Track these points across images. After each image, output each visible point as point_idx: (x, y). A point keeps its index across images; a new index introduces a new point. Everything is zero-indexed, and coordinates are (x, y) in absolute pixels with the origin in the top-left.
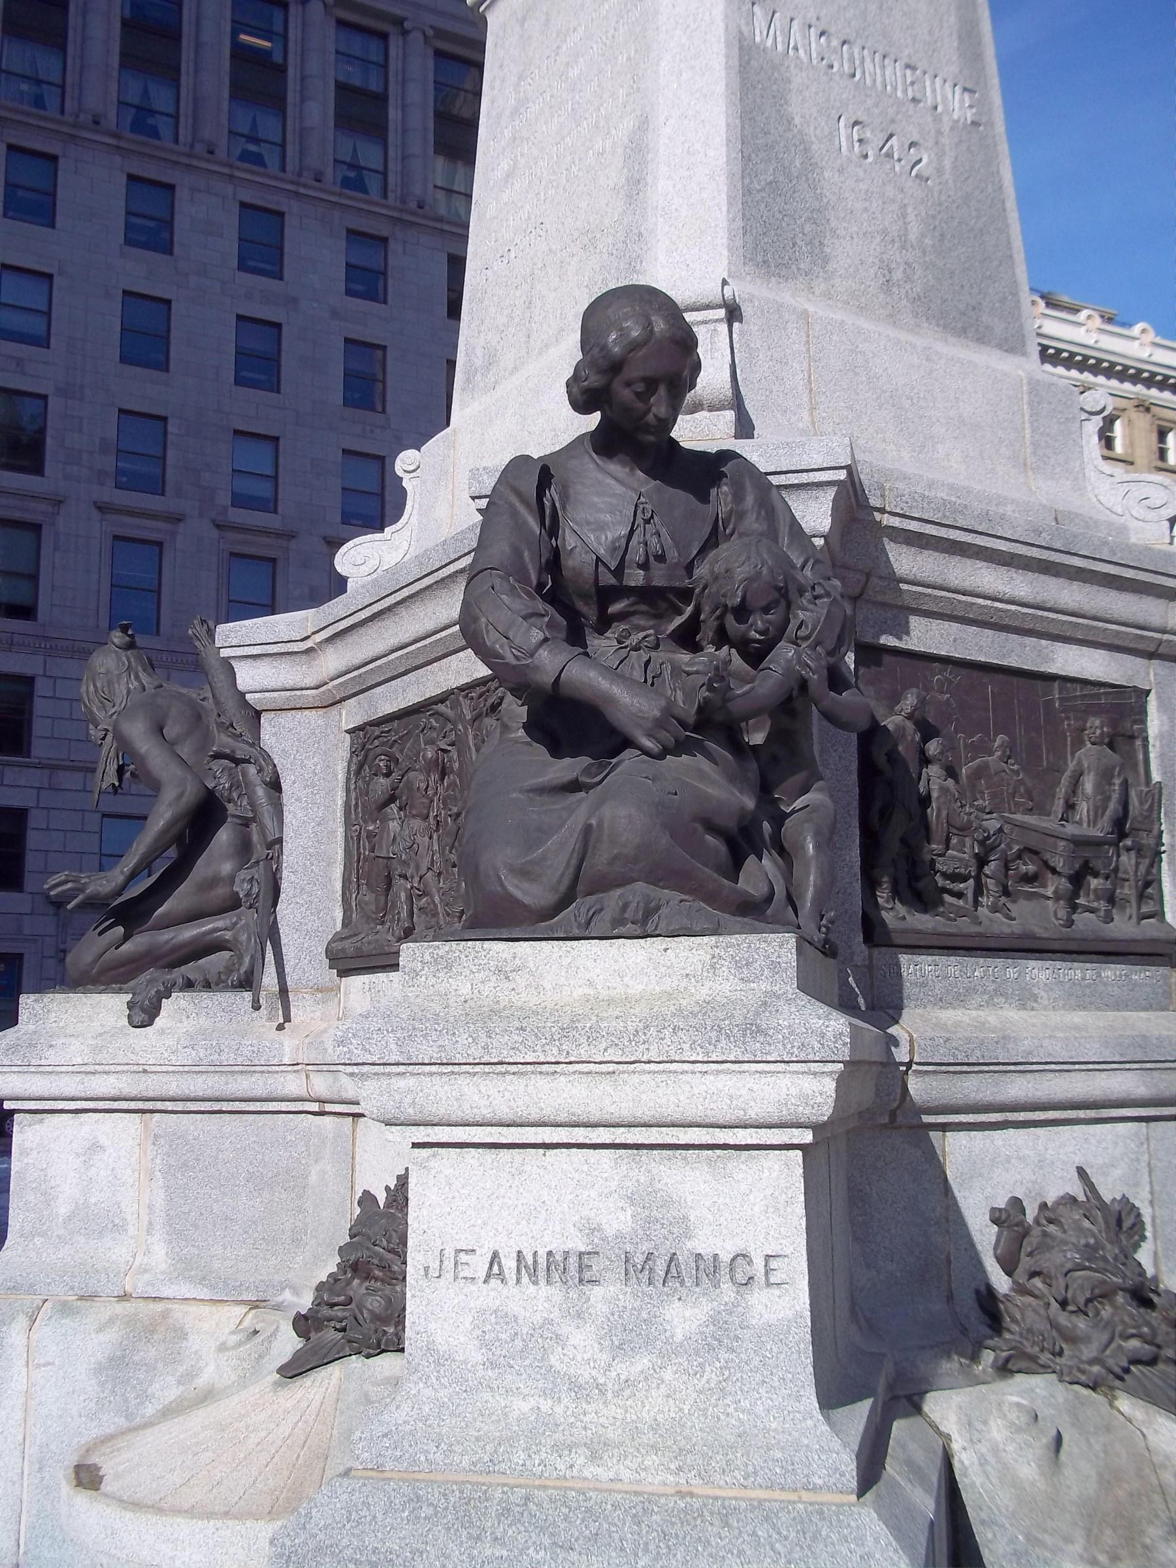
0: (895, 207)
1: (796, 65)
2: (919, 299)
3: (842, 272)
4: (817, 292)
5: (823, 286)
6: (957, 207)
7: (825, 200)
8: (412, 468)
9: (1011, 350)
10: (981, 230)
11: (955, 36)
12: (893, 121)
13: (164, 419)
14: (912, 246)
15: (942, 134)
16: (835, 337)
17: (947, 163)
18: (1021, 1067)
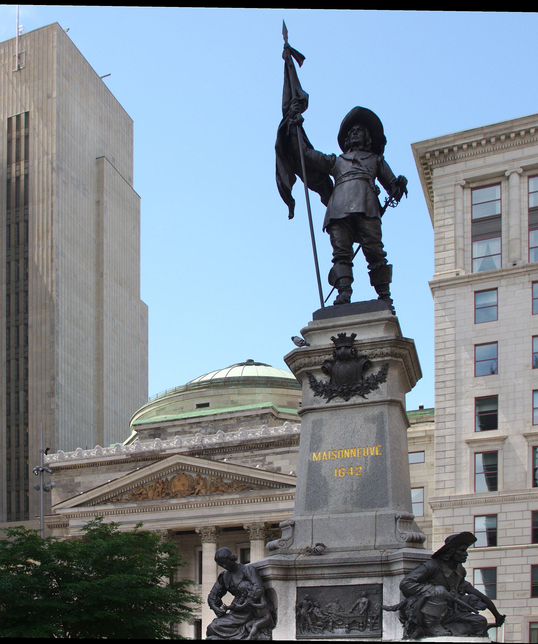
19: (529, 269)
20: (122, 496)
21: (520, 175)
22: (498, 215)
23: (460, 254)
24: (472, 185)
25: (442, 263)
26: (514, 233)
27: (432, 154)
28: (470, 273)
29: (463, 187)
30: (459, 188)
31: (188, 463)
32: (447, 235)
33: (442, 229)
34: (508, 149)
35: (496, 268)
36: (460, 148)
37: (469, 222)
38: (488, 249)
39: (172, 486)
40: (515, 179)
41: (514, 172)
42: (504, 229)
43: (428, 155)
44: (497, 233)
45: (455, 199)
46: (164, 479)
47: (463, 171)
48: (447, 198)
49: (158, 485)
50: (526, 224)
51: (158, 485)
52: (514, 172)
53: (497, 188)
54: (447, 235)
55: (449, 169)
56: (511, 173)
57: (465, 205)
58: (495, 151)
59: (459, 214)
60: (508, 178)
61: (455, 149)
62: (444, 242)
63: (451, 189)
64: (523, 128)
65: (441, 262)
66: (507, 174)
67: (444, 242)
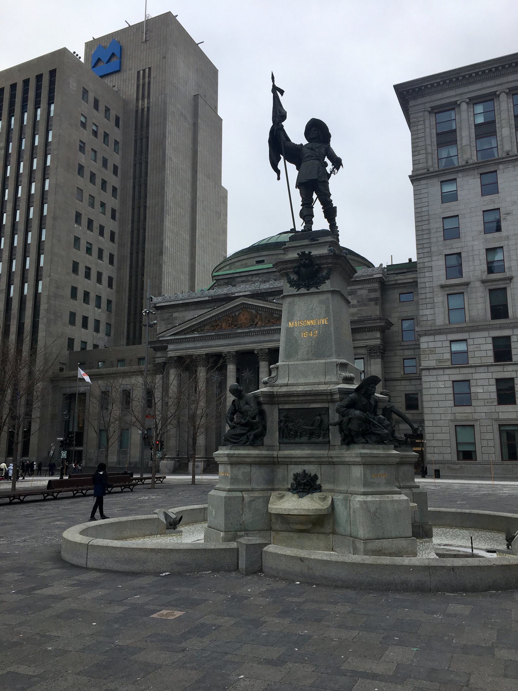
18: (294, 458)
19: (477, 165)
20: (204, 327)
21: (468, 103)
22: (454, 129)
23: (430, 156)
24: (435, 111)
25: (418, 163)
26: (465, 141)
27: (408, 91)
28: (437, 169)
29: (430, 112)
30: (426, 113)
31: (249, 303)
32: (420, 144)
33: (417, 140)
34: (458, 87)
35: (454, 165)
36: (426, 87)
37: (435, 135)
38: (449, 153)
39: (239, 319)
40: (464, 106)
41: (463, 102)
42: (458, 139)
43: (405, 93)
44: (453, 142)
45: (424, 120)
46: (233, 315)
47: (429, 102)
48: (419, 120)
49: (229, 319)
50: (473, 135)
51: (229, 319)
52: (463, 102)
53: (453, 113)
54: (420, 144)
55: (420, 101)
56: (461, 102)
57: (432, 123)
58: (450, 89)
59: (428, 130)
60: (459, 105)
61: (423, 88)
62: (418, 149)
63: (421, 114)
64: (467, 73)
65: (417, 162)
66: (458, 102)
67: (418, 149)
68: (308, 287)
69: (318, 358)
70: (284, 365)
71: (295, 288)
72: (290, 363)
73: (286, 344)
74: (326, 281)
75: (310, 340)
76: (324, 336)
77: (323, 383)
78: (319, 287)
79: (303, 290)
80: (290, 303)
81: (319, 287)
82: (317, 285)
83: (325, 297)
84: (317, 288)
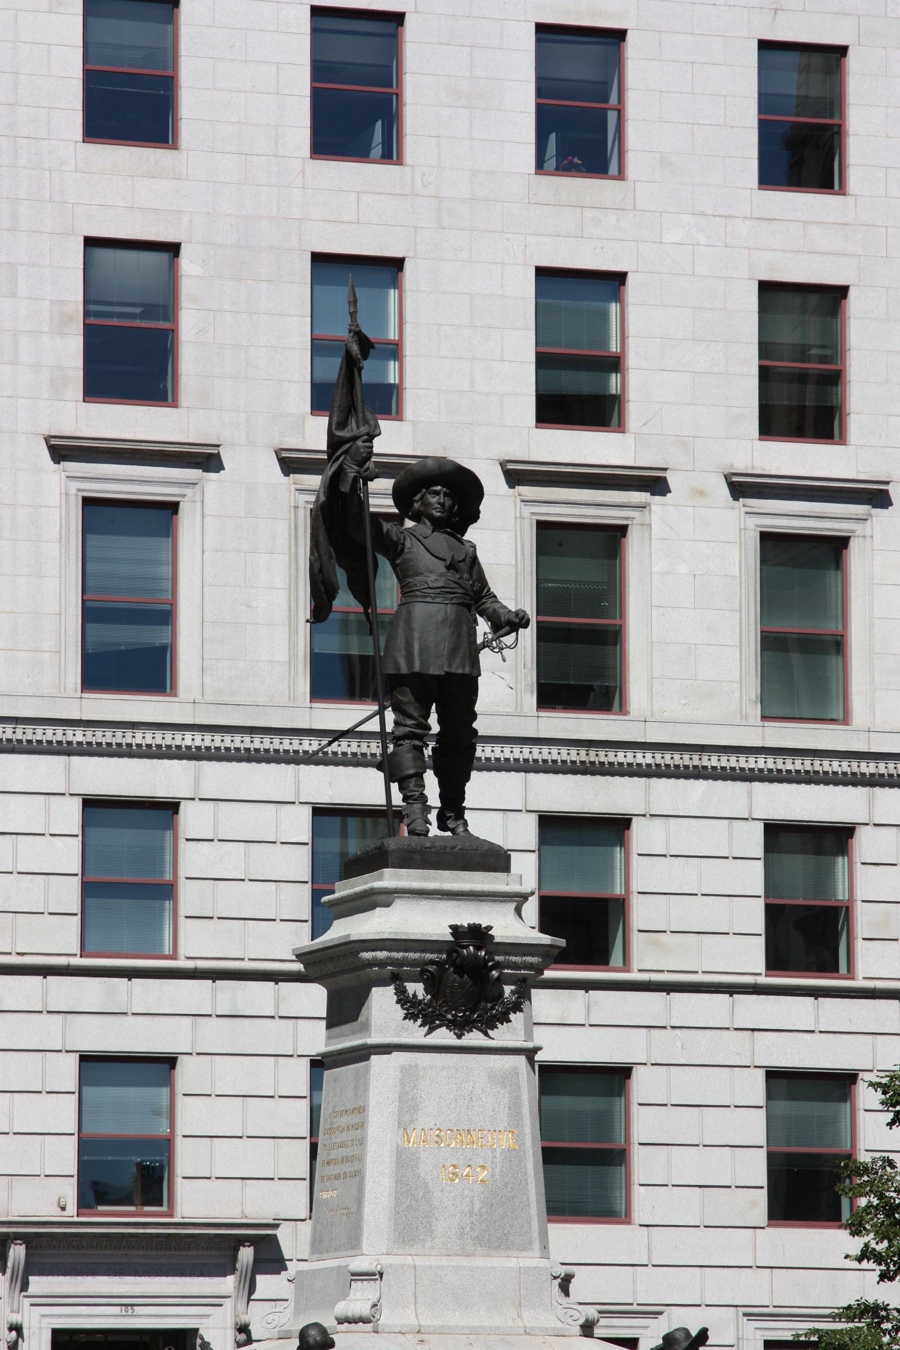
0: (468, 1199)
1: (423, 1150)
2: (477, 1237)
3: (440, 1235)
4: (427, 1248)
5: (430, 1244)
6: (501, 1190)
7: (433, 1206)
8: (291, 1279)
9: (525, 1249)
10: (513, 1197)
11: (507, 1108)
12: (470, 1159)
13: (173, 249)
14: (476, 1215)
15: (495, 1157)
16: (427, 1272)
17: (497, 1170)
68: (460, 1027)
69: (492, 1252)
70: (403, 1266)
71: (419, 1021)
72: (419, 1261)
73: (397, 1199)
74: (512, 1016)
75: (466, 1192)
76: (506, 1185)
77: (522, 1332)
78: (489, 1032)
79: (444, 1036)
80: (405, 1070)
81: (489, 1032)
82: (488, 1024)
83: (507, 1066)
84: (486, 1034)
